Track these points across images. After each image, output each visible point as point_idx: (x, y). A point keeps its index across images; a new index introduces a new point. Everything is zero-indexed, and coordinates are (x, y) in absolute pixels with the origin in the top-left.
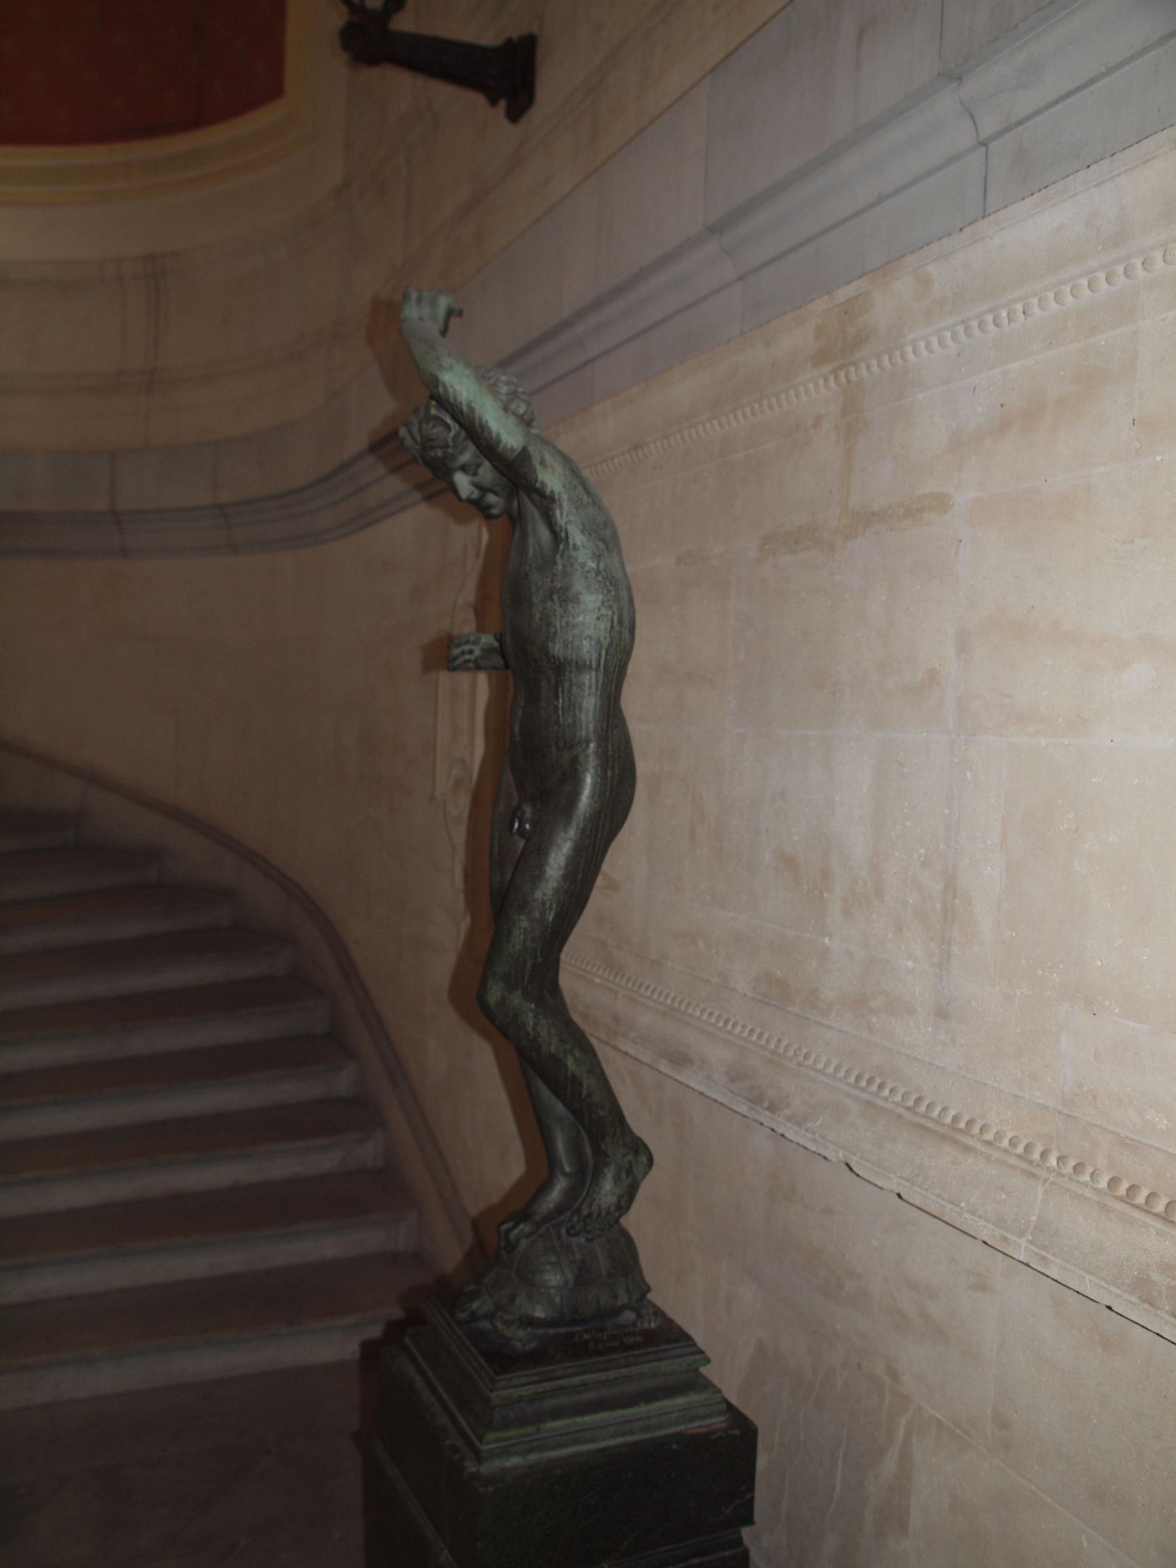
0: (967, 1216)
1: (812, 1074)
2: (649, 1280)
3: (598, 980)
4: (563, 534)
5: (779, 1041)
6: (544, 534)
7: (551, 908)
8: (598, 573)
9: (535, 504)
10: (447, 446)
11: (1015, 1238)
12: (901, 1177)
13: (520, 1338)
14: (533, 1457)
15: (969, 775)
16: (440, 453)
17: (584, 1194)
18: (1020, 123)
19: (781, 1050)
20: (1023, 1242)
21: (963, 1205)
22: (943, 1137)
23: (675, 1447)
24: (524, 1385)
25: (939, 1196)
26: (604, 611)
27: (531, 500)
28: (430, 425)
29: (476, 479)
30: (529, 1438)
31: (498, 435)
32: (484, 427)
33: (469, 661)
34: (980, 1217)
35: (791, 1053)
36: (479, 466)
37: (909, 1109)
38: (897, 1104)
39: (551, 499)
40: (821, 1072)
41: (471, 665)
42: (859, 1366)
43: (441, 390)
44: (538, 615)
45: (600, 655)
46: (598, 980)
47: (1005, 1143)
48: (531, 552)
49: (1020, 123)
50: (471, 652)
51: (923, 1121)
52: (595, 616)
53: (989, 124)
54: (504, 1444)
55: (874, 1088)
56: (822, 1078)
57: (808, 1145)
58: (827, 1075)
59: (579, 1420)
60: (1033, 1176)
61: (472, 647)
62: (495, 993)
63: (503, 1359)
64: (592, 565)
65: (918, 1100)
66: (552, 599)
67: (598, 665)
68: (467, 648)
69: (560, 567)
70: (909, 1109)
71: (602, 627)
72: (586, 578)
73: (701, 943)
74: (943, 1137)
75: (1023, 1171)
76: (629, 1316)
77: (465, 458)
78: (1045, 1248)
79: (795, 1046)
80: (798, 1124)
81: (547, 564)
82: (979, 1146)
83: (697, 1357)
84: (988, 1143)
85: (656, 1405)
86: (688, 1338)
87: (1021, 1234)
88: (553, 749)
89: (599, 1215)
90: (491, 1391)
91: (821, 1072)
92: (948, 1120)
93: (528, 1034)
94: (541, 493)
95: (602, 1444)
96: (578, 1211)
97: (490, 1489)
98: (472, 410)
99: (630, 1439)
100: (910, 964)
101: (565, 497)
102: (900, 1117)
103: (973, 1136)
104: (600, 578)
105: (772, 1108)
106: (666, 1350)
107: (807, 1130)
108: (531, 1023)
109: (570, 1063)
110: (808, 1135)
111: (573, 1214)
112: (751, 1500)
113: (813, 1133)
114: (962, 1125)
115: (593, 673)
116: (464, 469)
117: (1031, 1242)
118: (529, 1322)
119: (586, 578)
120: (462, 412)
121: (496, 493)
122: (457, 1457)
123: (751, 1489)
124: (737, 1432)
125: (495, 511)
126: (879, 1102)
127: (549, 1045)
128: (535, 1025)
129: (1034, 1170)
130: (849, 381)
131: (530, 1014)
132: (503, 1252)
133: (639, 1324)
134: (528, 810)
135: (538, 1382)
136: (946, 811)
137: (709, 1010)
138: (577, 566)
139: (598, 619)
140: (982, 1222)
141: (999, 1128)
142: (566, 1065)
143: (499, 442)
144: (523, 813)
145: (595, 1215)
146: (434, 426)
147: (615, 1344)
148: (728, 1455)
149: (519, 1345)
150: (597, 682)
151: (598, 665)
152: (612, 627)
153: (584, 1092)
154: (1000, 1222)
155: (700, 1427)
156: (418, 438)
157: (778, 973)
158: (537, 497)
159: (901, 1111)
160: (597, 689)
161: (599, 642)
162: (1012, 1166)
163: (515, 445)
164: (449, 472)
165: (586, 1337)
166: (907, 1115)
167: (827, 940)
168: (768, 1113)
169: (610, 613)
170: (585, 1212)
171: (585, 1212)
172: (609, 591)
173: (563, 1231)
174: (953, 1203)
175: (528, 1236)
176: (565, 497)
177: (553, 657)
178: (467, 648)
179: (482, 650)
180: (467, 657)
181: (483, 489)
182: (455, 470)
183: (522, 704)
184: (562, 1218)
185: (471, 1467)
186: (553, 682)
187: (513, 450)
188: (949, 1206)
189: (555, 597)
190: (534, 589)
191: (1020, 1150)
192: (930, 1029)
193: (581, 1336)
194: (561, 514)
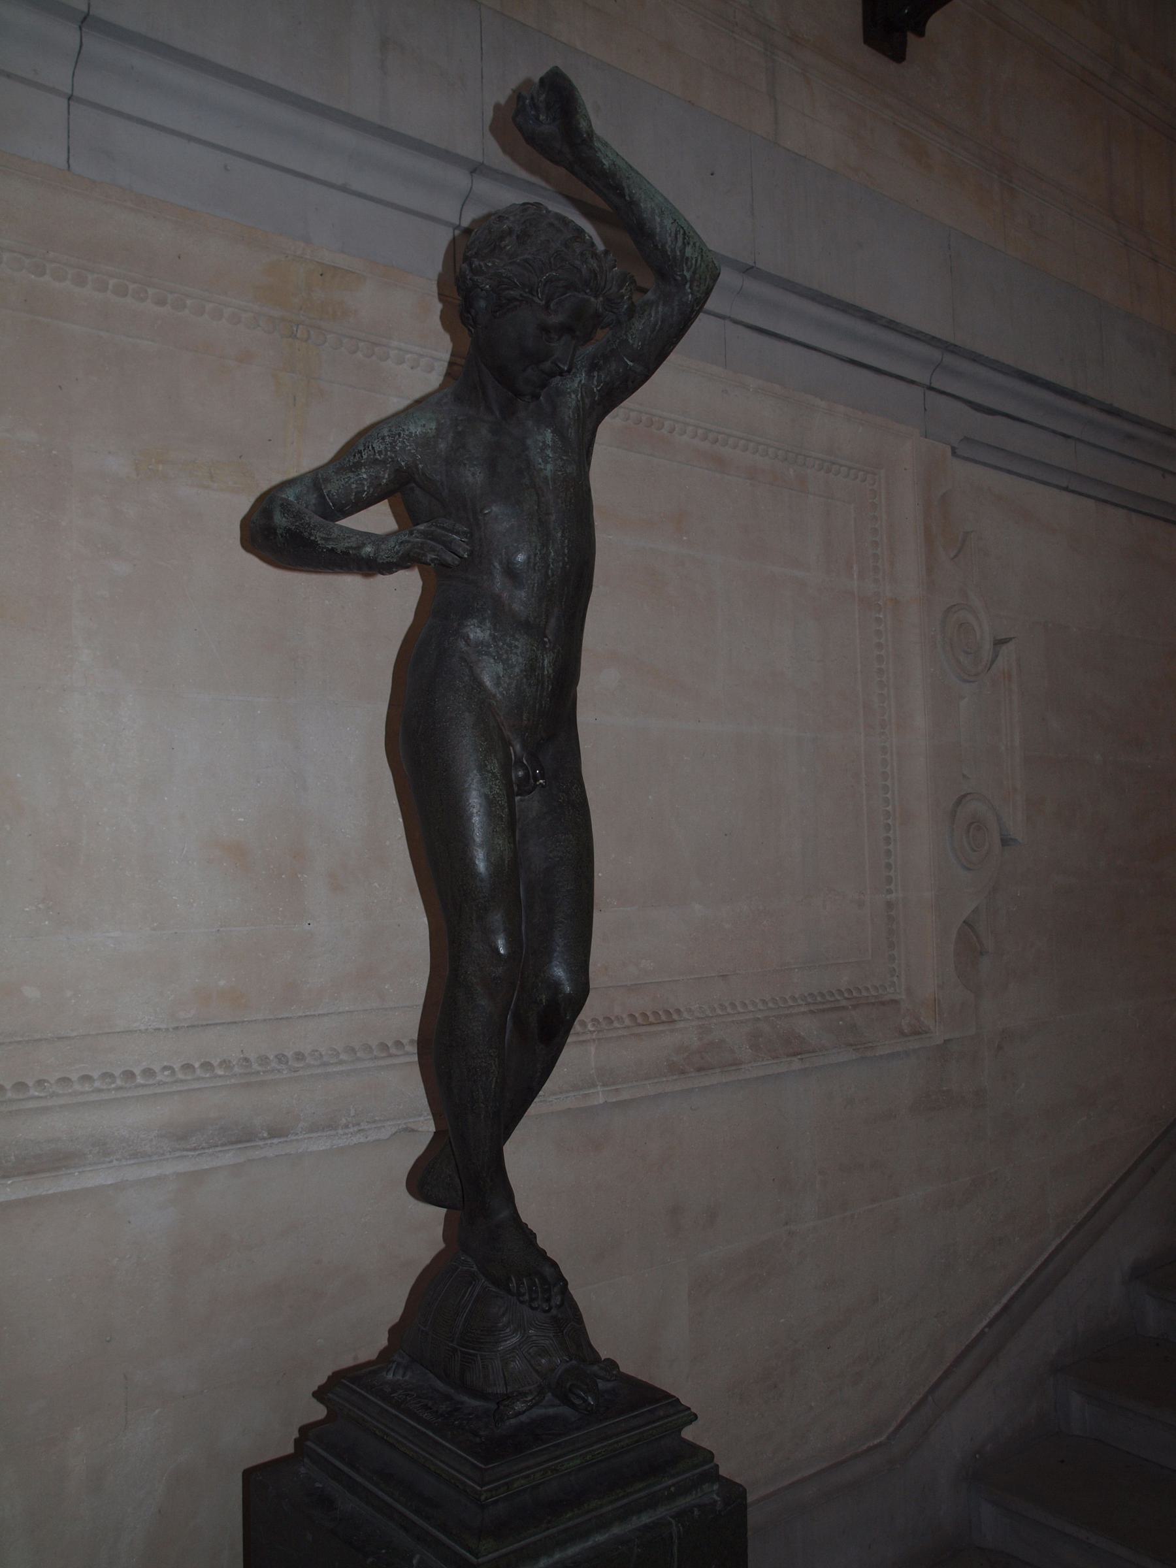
87: (594, 1085)
107: (347, 1126)
113: (359, 1124)
117: (604, 1085)
122: (696, 1512)
129: (581, 1038)
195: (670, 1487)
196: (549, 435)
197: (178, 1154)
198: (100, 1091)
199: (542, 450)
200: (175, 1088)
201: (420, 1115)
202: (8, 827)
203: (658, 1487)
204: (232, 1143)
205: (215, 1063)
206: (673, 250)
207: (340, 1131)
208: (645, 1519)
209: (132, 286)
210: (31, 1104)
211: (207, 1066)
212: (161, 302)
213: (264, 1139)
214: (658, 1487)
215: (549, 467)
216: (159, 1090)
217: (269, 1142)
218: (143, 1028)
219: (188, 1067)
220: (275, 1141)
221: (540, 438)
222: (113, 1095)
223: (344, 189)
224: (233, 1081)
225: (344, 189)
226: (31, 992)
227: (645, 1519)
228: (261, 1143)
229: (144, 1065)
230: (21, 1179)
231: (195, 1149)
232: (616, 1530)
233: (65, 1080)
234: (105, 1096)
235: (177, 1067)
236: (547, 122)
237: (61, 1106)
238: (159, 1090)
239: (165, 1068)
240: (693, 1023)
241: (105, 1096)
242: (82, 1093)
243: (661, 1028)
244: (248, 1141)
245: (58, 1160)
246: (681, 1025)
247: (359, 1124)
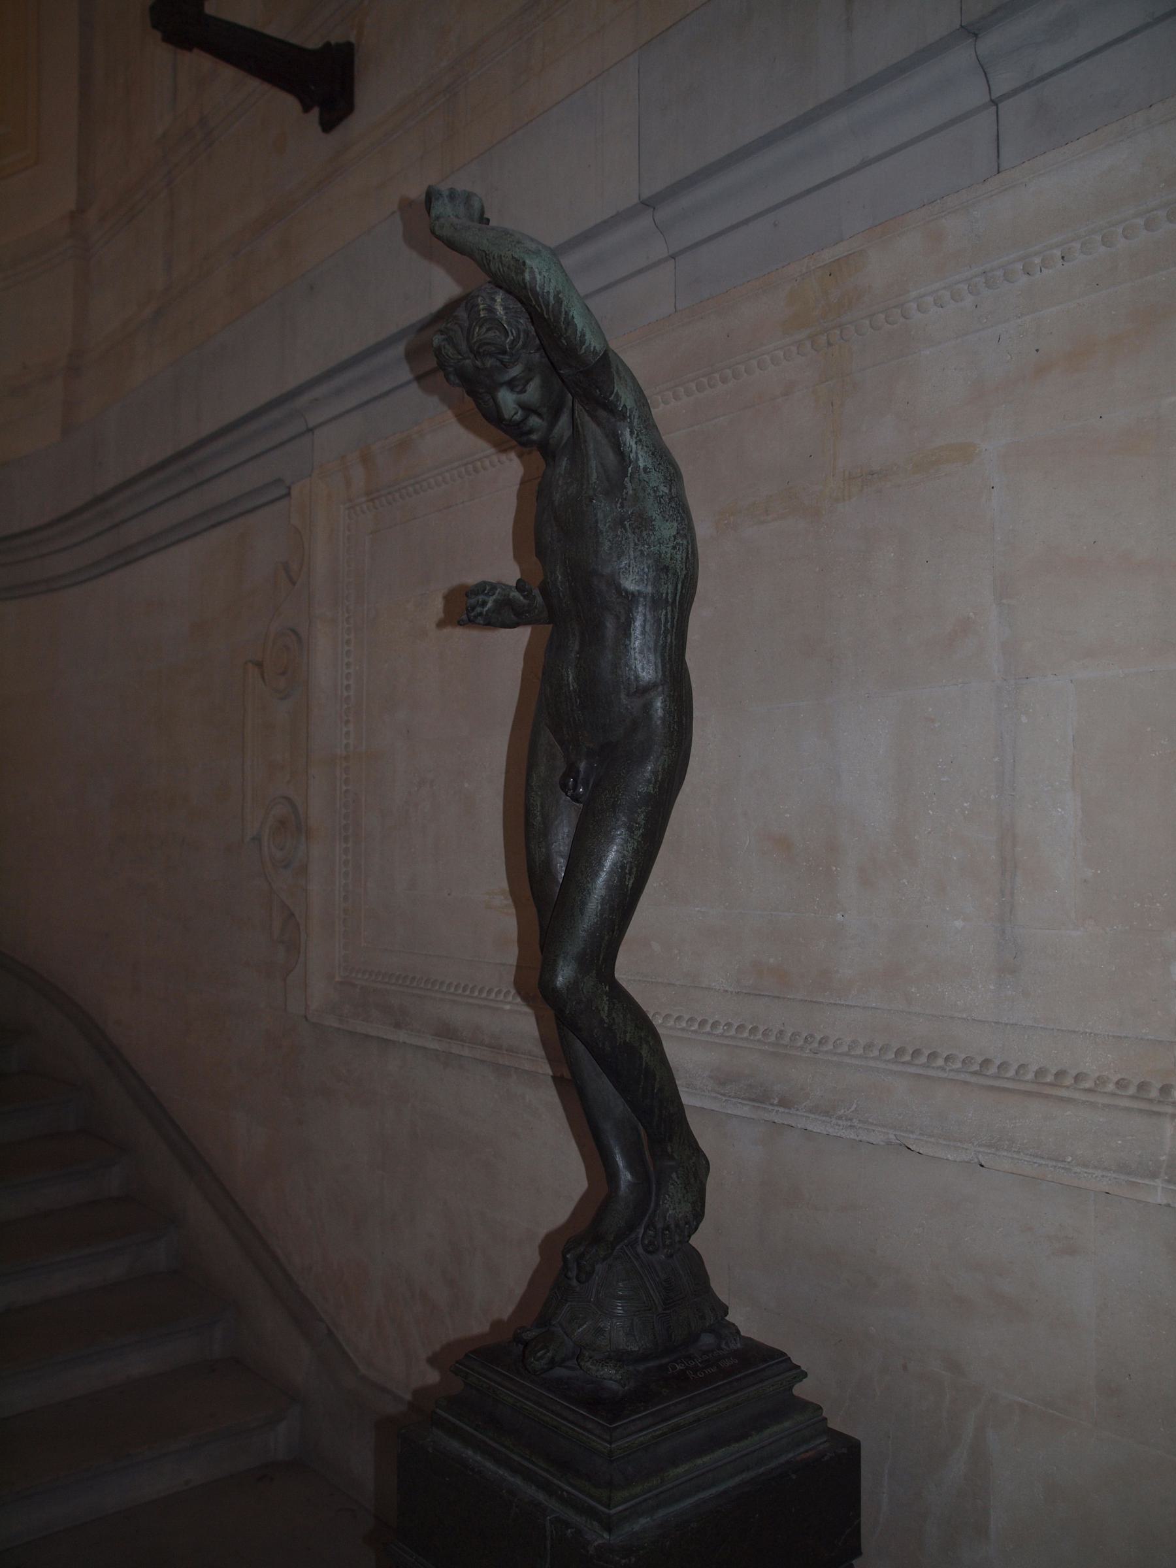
0: (1078, 1170)
1: (835, 1058)
2: (723, 1298)
3: (508, 1007)
4: (632, 456)
5: (781, 1032)
6: (611, 457)
7: (630, 874)
8: (671, 499)
9: (599, 424)
10: (504, 352)
11: (1147, 1182)
12: (980, 1146)
13: (611, 1377)
14: (660, 1514)
15: (1024, 719)
16: (489, 362)
17: (652, 1205)
18: (1042, 79)
19: (786, 1040)
20: (1159, 1183)
21: (1070, 1159)
22: (1028, 1094)
23: (794, 1477)
24: (641, 1430)
25: (1036, 1156)
26: (679, 541)
27: (594, 418)
28: (484, 329)
29: (524, 397)
30: (655, 1492)
31: (583, 335)
32: (569, 322)
33: (480, 614)
34: (1095, 1167)
35: (800, 1043)
36: (527, 382)
37: (975, 1073)
38: (958, 1071)
39: (623, 416)
40: (847, 1054)
41: (480, 620)
42: (905, 1367)
43: (527, 276)
44: (607, 544)
45: (676, 589)
46: (508, 1007)
47: (1111, 1087)
48: (595, 476)
49: (1042, 79)
50: (484, 604)
51: (997, 1083)
52: (671, 544)
53: (1003, 81)
54: (632, 1503)
55: (923, 1059)
56: (847, 1060)
57: (843, 1133)
58: (856, 1057)
59: (699, 1461)
60: (1158, 1114)
61: (486, 598)
62: (563, 977)
63: (605, 1406)
64: (664, 489)
65: (986, 1062)
66: (624, 527)
67: (674, 600)
68: (481, 598)
69: (631, 492)
70: (975, 1073)
71: (678, 557)
72: (660, 503)
73: (656, 946)
74: (1028, 1094)
75: (1140, 1111)
76: (707, 1340)
77: (515, 371)
79: (804, 1035)
80: (826, 1113)
81: (614, 488)
82: (1077, 1095)
83: (794, 1372)
84: (1089, 1090)
85: (767, 1432)
86: (783, 1354)
87: (1154, 1175)
88: (623, 696)
89: (677, 1226)
90: (610, 1443)
91: (847, 1054)
92: (1030, 1076)
93: (602, 1020)
94: (611, 408)
95: (722, 1487)
96: (651, 1225)
97: (633, 1559)
98: (559, 301)
99: (746, 1476)
100: (959, 924)
101: (636, 413)
102: (966, 1083)
103: (1068, 1087)
104: (673, 505)
105: (784, 1103)
106: (764, 1369)
107: (840, 1118)
108: (606, 1008)
109: (644, 1052)
110: (840, 1122)
111: (647, 1227)
112: (859, 1524)
113: (851, 1120)
114: (1050, 1078)
115: (669, 608)
116: (511, 385)
117: (1169, 1181)
118: (619, 1358)
119: (660, 503)
120: (547, 305)
121: (540, 415)
123: (859, 1515)
124: (844, 1450)
125: (534, 437)
126: (931, 1072)
127: (625, 1032)
128: (610, 1010)
129: (1156, 1108)
130: (829, 344)
131: (605, 998)
132: (574, 1282)
133: (723, 1346)
134: (582, 766)
135: (655, 1425)
136: (996, 759)
137: (676, 1015)
138: (649, 490)
139: (674, 548)
140: (1099, 1173)
141: (1097, 1074)
142: (641, 1057)
143: (583, 342)
144: (578, 772)
145: (673, 1226)
146: (488, 330)
147: (714, 1370)
148: (834, 1475)
149: (615, 1386)
150: (673, 618)
151: (674, 600)
152: (687, 558)
153: (657, 1086)
155: (807, 1451)
156: (464, 347)
157: (772, 960)
158: (602, 414)
159: (968, 1078)
160: (672, 627)
161: (675, 573)
162: (1128, 1110)
163: (598, 349)
164: (492, 390)
165: (678, 1367)
166: (973, 1079)
167: (839, 916)
168: (781, 1109)
169: (685, 542)
170: (660, 1225)
171: (660, 1225)
172: (683, 519)
173: (640, 1249)
174: (1057, 1160)
175: (604, 1259)
176: (636, 413)
177: (626, 592)
178: (481, 598)
179: (496, 601)
180: (479, 609)
181: (528, 409)
182: (502, 384)
183: (577, 648)
184: (633, 1236)
185: (597, 1537)
186: (623, 619)
187: (595, 352)
188: (1051, 1163)
189: (627, 524)
190: (600, 515)
191: (1132, 1090)
192: (992, 987)
193: (674, 1368)
194: (632, 433)
195: (563, 1490)
201: (912, 1132)
203: (556, 1481)
207: (834, 1121)
208: (541, 1497)
214: (556, 1481)
223: (866, 164)
225: (866, 164)
227: (541, 1497)
232: (518, 1481)
247: (851, 1120)
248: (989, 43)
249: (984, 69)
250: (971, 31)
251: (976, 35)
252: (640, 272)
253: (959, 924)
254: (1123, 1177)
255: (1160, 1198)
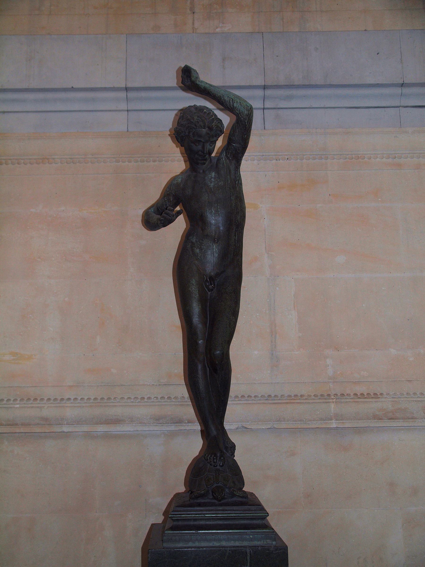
11: (330, 422)
15: (277, 288)
18: (279, 108)
20: (333, 421)
22: (287, 403)
49: (279, 108)
74: (287, 403)
78: (341, 420)
82: (302, 401)
87: (331, 419)
117: (336, 420)
136: (268, 300)
154: (321, 419)
157: (176, 371)
166: (266, 402)
188: (299, 422)
196: (213, 174)
197: (155, 424)
198: (132, 402)
199: (210, 179)
200: (157, 404)
201: (248, 422)
202: (108, 321)
204: (174, 423)
205: (173, 397)
206: (230, 106)
209: (145, 159)
210: (111, 404)
211: (169, 398)
212: (154, 161)
213: (185, 423)
215: (212, 184)
216: (151, 404)
217: (188, 424)
218: (148, 384)
219: (162, 398)
220: (190, 424)
221: (210, 176)
222: (137, 404)
224: (177, 403)
226: (114, 371)
228: (185, 424)
229: (148, 396)
230: (105, 425)
231: (161, 423)
233: (122, 398)
234: (134, 404)
235: (159, 397)
236: (188, 80)
237: (120, 406)
238: (151, 404)
239: (155, 397)
240: (390, 400)
241: (134, 404)
242: (127, 402)
243: (371, 400)
244: (181, 423)
245: (117, 421)
246: (383, 400)
248: (268, 92)
249: (264, 99)
250: (265, 87)
251: (264, 89)
252: (110, 111)
253: (256, 352)
254: (322, 422)
255: (334, 426)
